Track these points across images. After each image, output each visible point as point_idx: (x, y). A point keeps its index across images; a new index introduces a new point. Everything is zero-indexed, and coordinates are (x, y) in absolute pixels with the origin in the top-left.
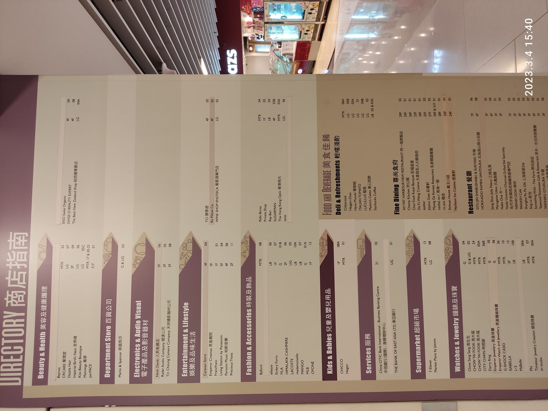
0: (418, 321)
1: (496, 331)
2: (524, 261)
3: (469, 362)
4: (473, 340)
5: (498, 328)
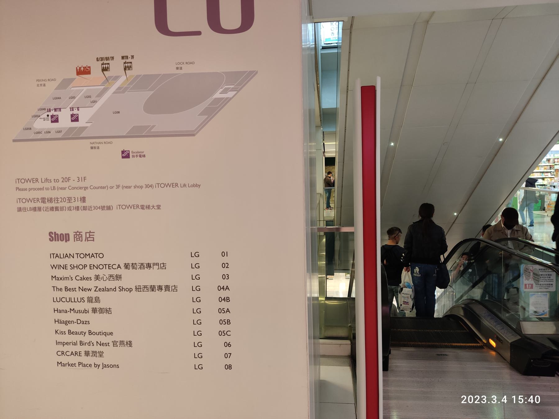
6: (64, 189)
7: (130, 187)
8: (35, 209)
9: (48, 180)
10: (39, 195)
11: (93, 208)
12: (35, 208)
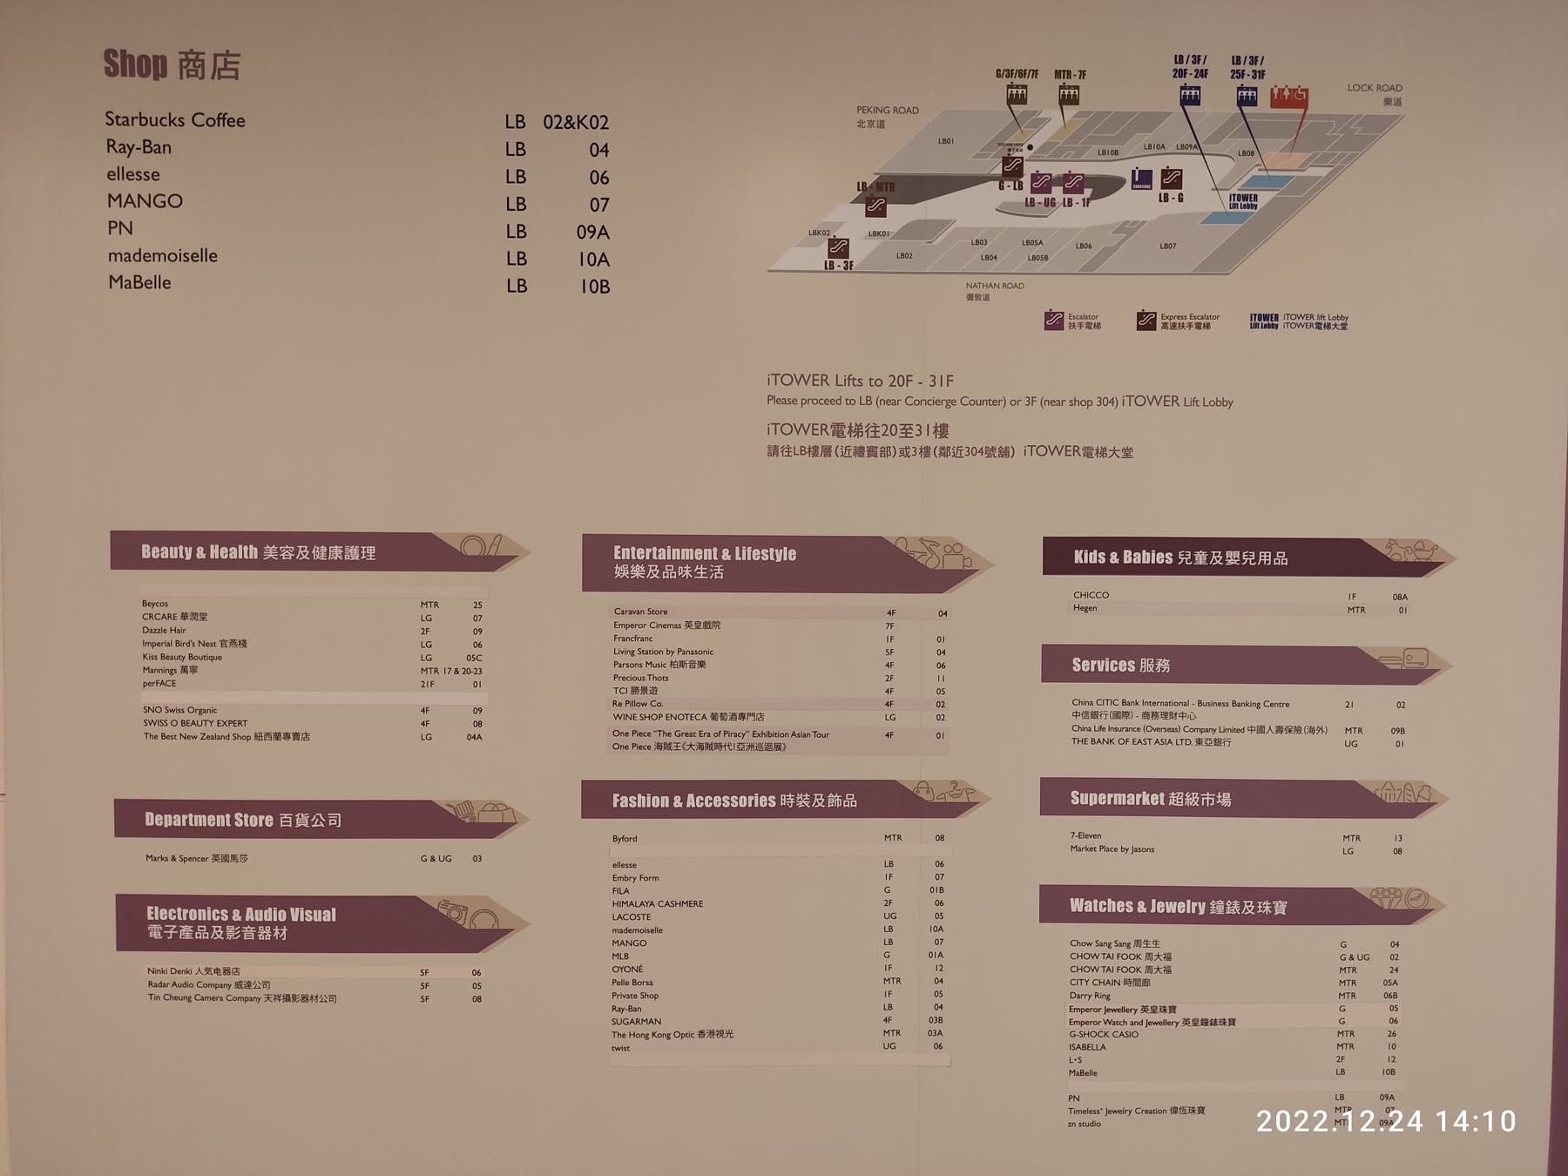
0: (1200, 802)
1: (1169, 1017)
2: (1342, 1097)
3: (1094, 944)
4: (1149, 956)
5: (1175, 1024)
6: (896, 403)
7: (1060, 403)
8: (814, 451)
9: (854, 379)
10: (830, 415)
11: (965, 452)
12: (816, 447)
